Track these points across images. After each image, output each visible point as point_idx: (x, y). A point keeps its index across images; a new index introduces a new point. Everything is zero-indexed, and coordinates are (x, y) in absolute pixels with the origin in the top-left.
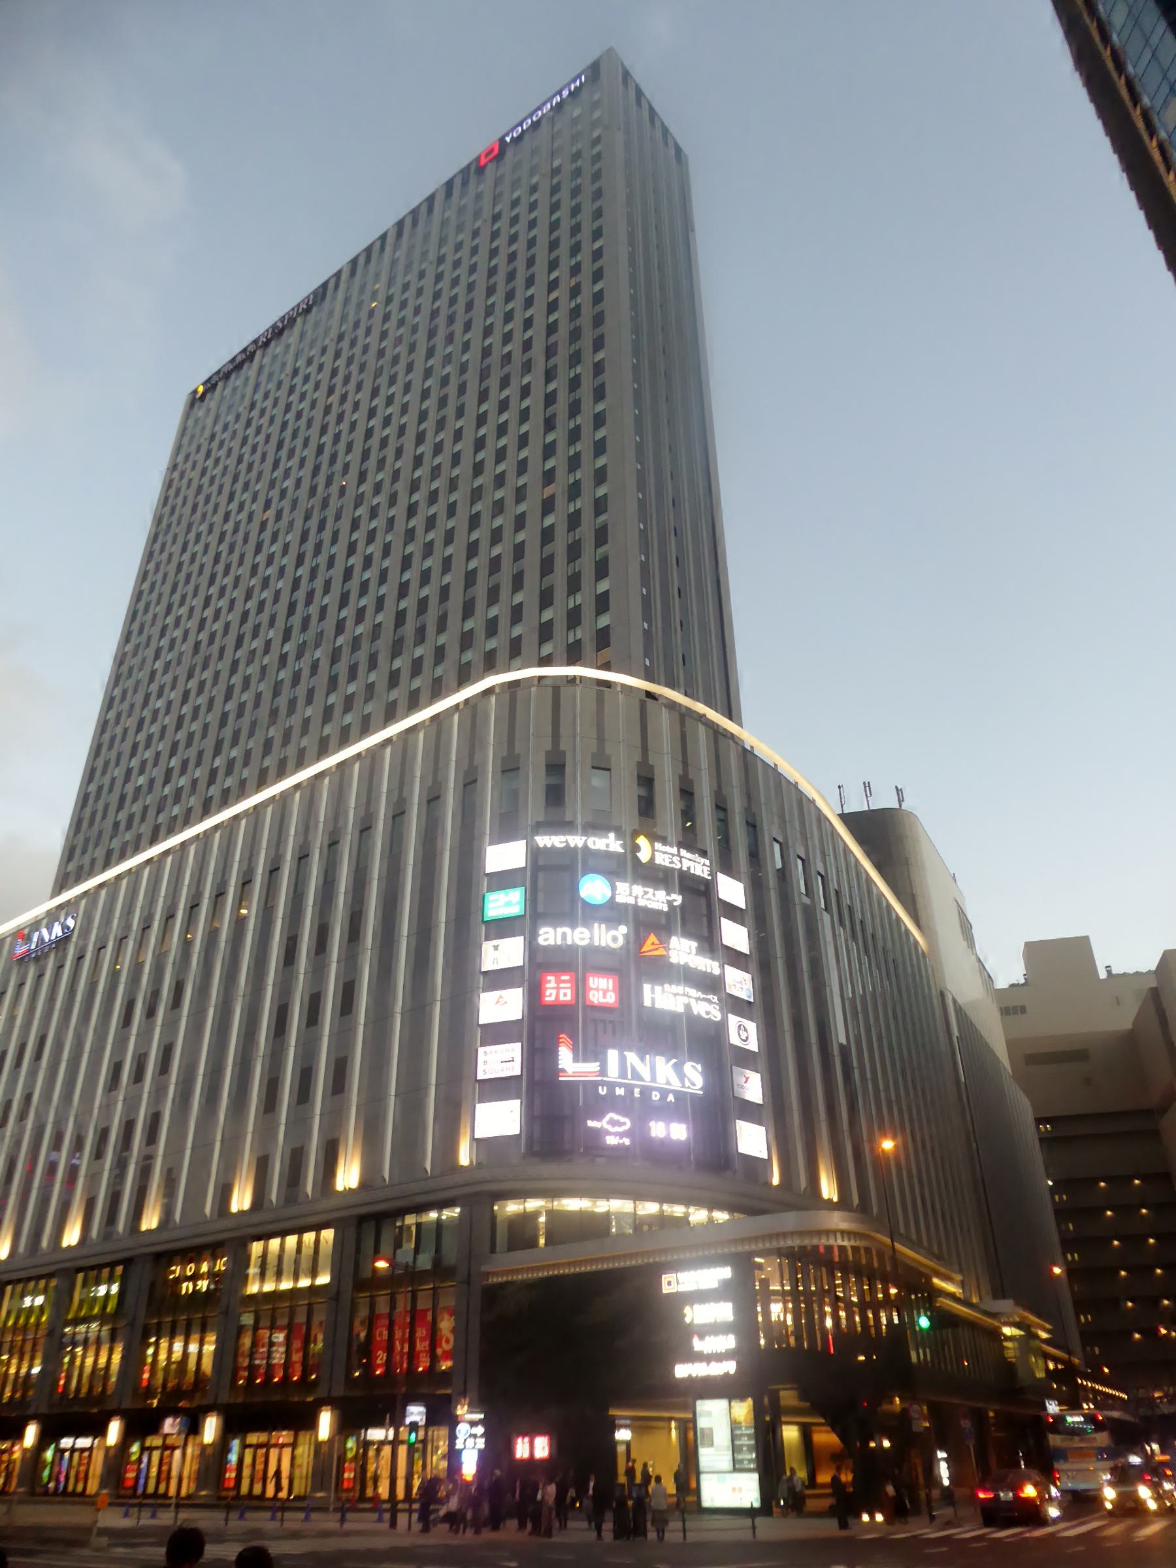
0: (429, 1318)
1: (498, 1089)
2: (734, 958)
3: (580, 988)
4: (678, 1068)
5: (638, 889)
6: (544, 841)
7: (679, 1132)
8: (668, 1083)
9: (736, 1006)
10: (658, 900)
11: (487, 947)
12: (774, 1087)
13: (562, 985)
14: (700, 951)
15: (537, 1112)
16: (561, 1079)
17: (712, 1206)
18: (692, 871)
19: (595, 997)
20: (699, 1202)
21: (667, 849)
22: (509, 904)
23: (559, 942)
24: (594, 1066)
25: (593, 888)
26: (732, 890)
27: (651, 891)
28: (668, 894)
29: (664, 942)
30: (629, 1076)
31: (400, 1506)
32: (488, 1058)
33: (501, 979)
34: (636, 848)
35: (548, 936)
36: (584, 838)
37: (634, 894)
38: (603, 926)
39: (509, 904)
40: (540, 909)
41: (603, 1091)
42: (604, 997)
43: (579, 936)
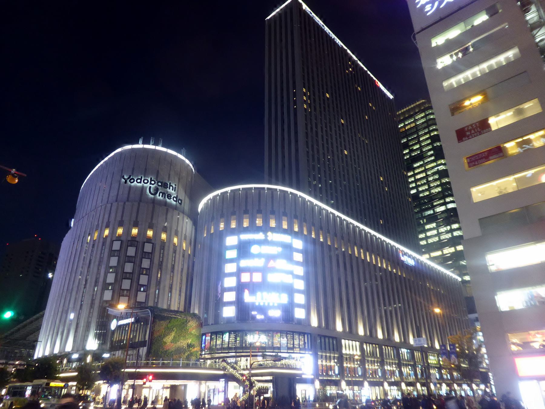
2: (298, 263)
9: (298, 277)
25: (255, 249)
33: (231, 275)
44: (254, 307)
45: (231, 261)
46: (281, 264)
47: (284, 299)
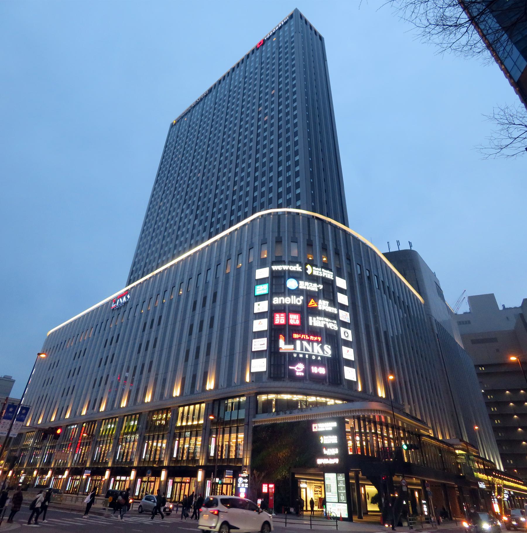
1: (259, 354)
2: (342, 307)
3: (287, 319)
4: (322, 348)
5: (307, 283)
6: (275, 268)
7: (322, 371)
8: (318, 353)
9: (344, 324)
10: (314, 287)
11: (256, 304)
12: (359, 353)
13: (281, 318)
14: (330, 305)
15: (272, 363)
16: (280, 351)
17: (335, 398)
18: (326, 277)
19: (292, 322)
20: (331, 397)
21: (317, 269)
22: (263, 290)
23: (280, 303)
24: (292, 347)
26: (341, 283)
27: (311, 284)
28: (318, 285)
29: (316, 302)
30: (304, 350)
32: (256, 343)
33: (261, 316)
34: (307, 269)
35: (277, 301)
36: (288, 266)
37: (306, 285)
38: (295, 297)
39: (263, 290)
40: (274, 291)
41: (295, 355)
42: (295, 321)
43: (287, 300)
44: (292, 359)
45: (261, 298)
46: (323, 305)
47: (328, 351)
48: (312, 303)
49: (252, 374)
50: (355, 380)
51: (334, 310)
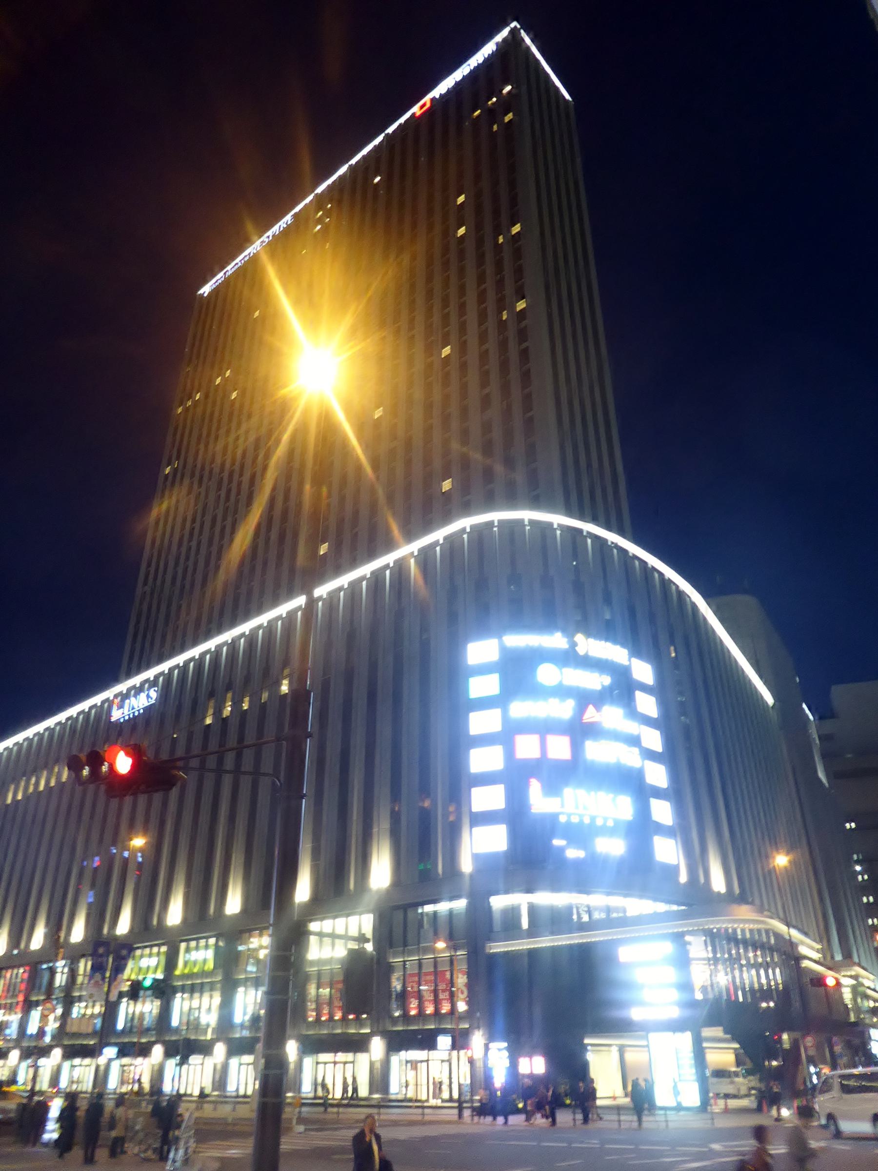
0: (448, 975)
2: (647, 721)
9: (650, 755)
29: (598, 708)
31: (465, 1105)
45: (484, 703)
48: (591, 714)
49: (476, 857)
50: (675, 863)
51: (633, 727)
